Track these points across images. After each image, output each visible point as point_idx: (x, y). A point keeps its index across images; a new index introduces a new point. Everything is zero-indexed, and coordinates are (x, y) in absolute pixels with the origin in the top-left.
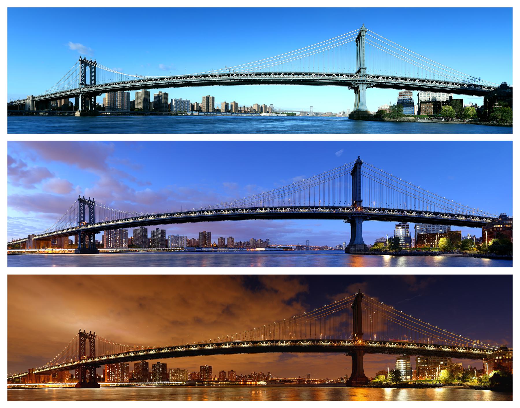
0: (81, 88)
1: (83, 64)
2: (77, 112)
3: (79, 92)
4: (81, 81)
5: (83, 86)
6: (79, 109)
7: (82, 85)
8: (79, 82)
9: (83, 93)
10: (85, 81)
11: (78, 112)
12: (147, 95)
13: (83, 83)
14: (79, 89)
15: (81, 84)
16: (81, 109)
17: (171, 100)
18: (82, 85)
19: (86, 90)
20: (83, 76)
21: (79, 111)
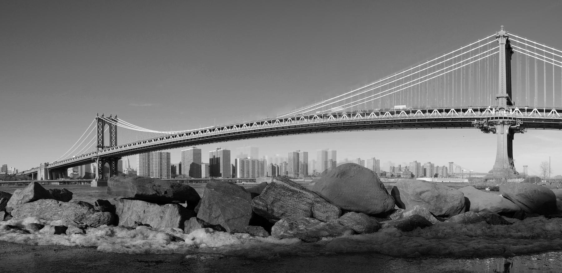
0: (98, 152)
1: (100, 123)
2: (94, 181)
3: (95, 157)
4: (98, 142)
5: (100, 149)
6: (96, 178)
7: (99, 147)
8: (96, 145)
9: (100, 158)
10: (103, 143)
11: (95, 181)
12: (197, 155)
13: (101, 146)
14: (95, 153)
15: (98, 147)
16: (98, 177)
17: (235, 159)
18: (99, 148)
19: (104, 153)
20: (100, 136)
21: (96, 180)
